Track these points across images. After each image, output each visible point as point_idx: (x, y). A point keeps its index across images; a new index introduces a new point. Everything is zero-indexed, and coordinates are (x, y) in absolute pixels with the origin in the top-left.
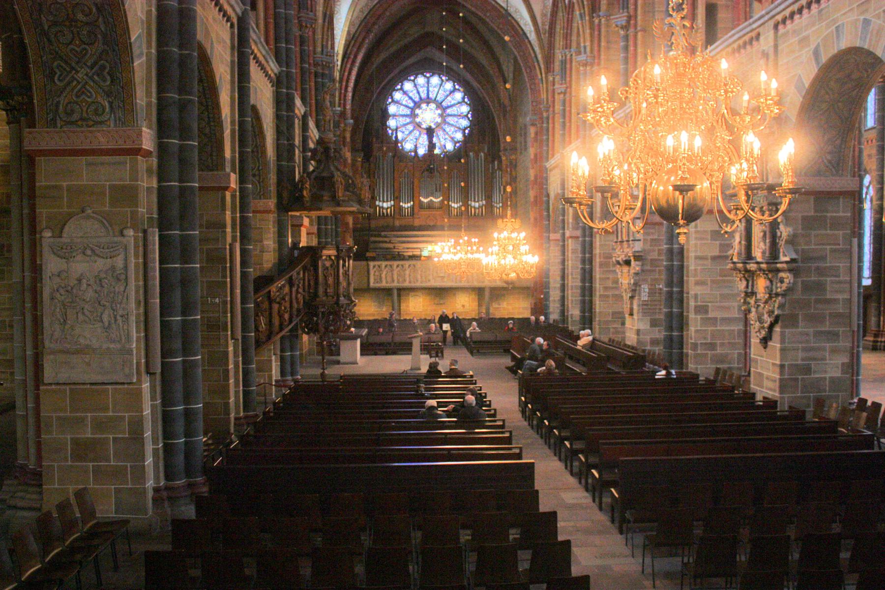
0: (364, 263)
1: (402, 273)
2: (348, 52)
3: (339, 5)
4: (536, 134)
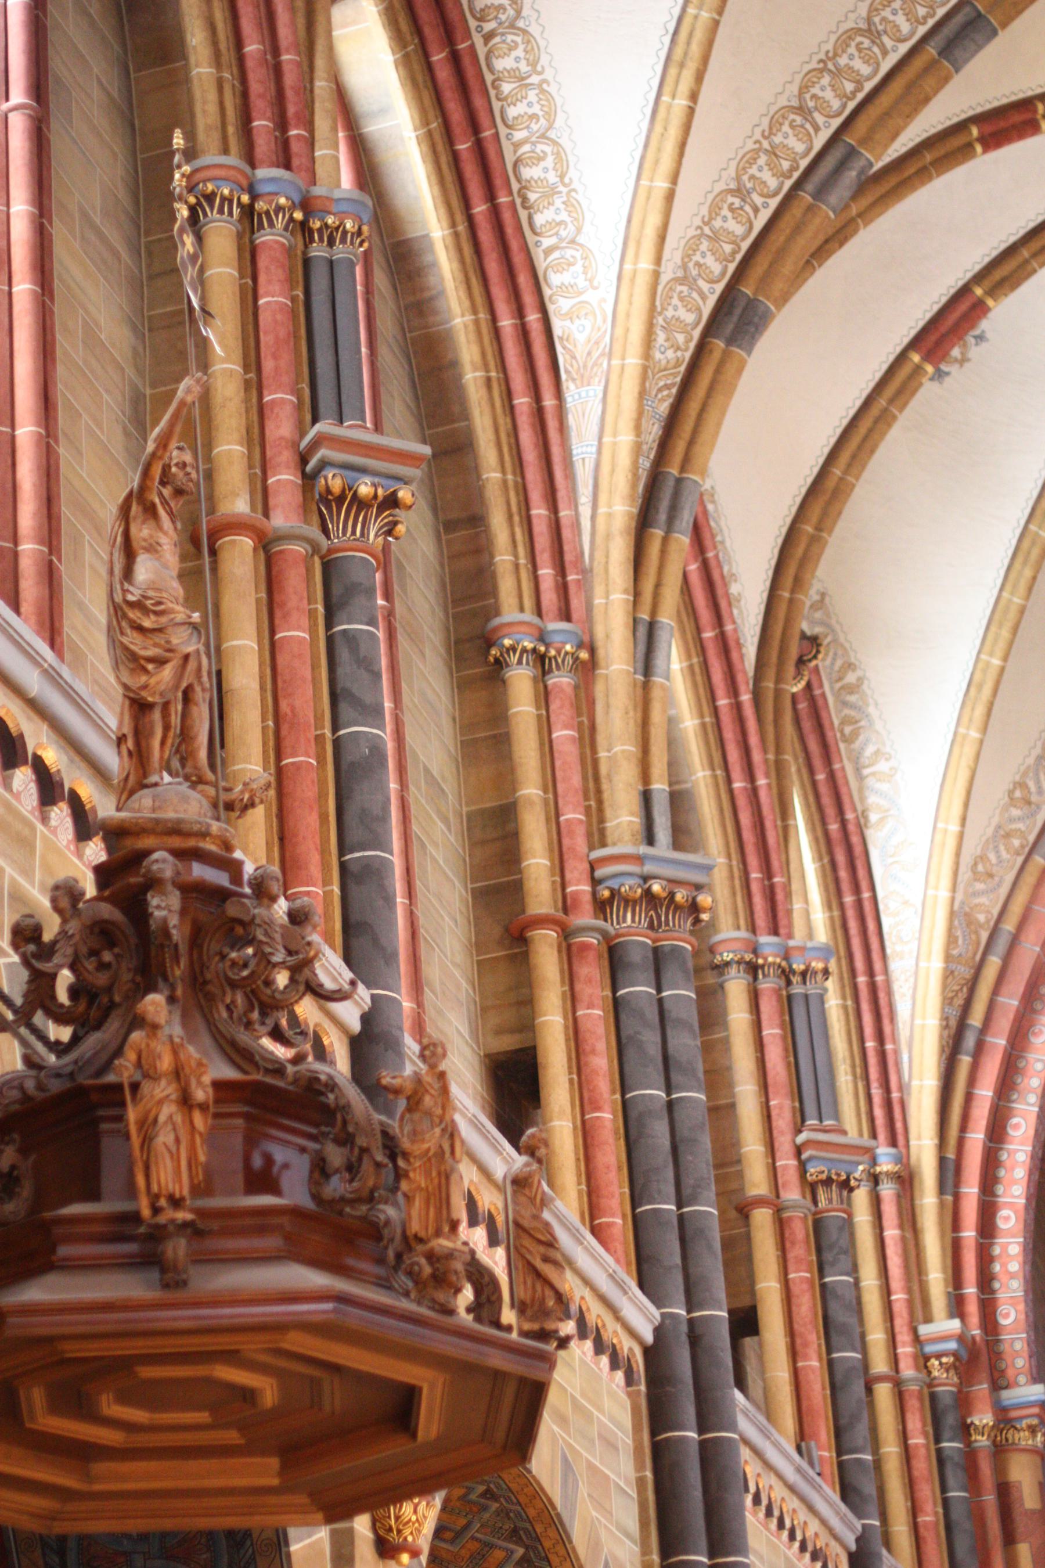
2: (976, 1020)
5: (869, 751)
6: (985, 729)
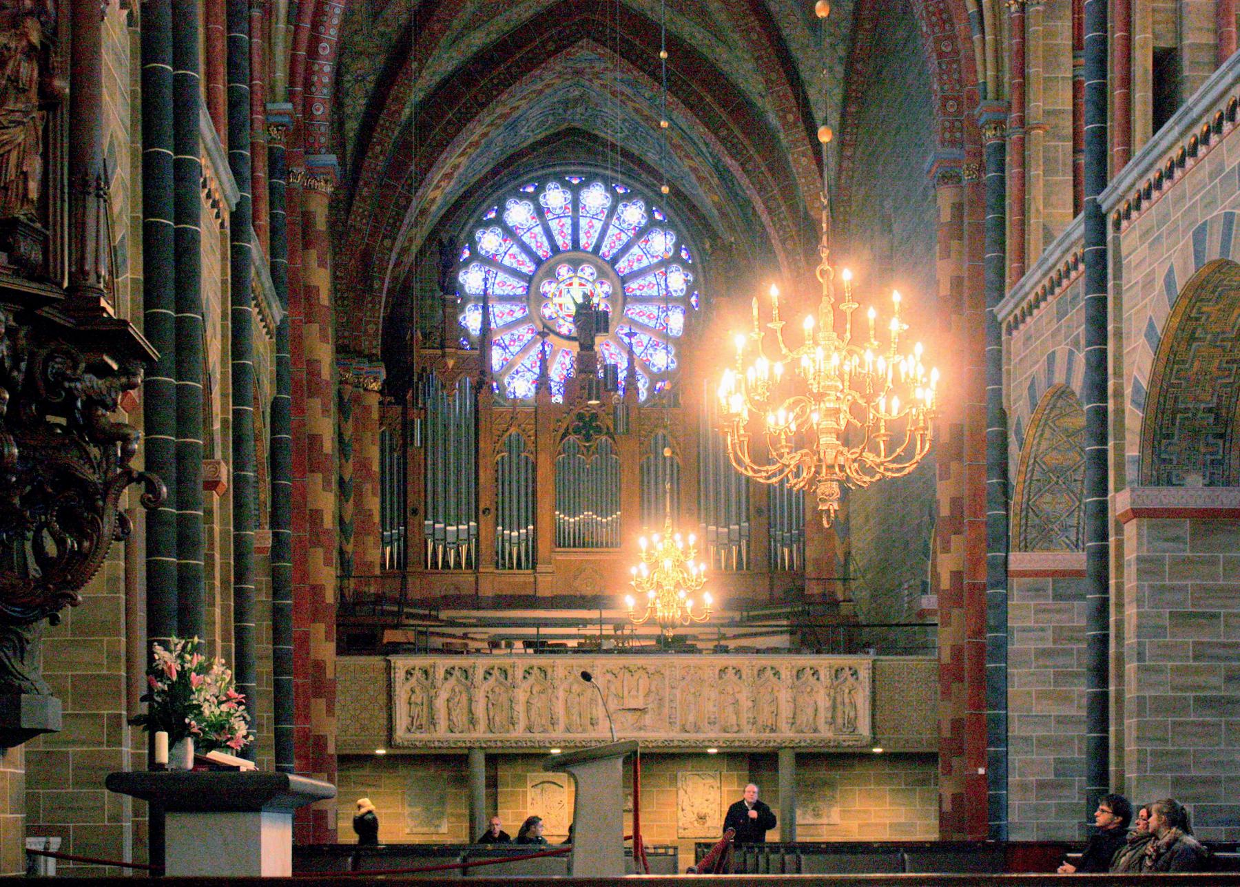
0: (377, 661)
1: (504, 698)
4: (958, 208)
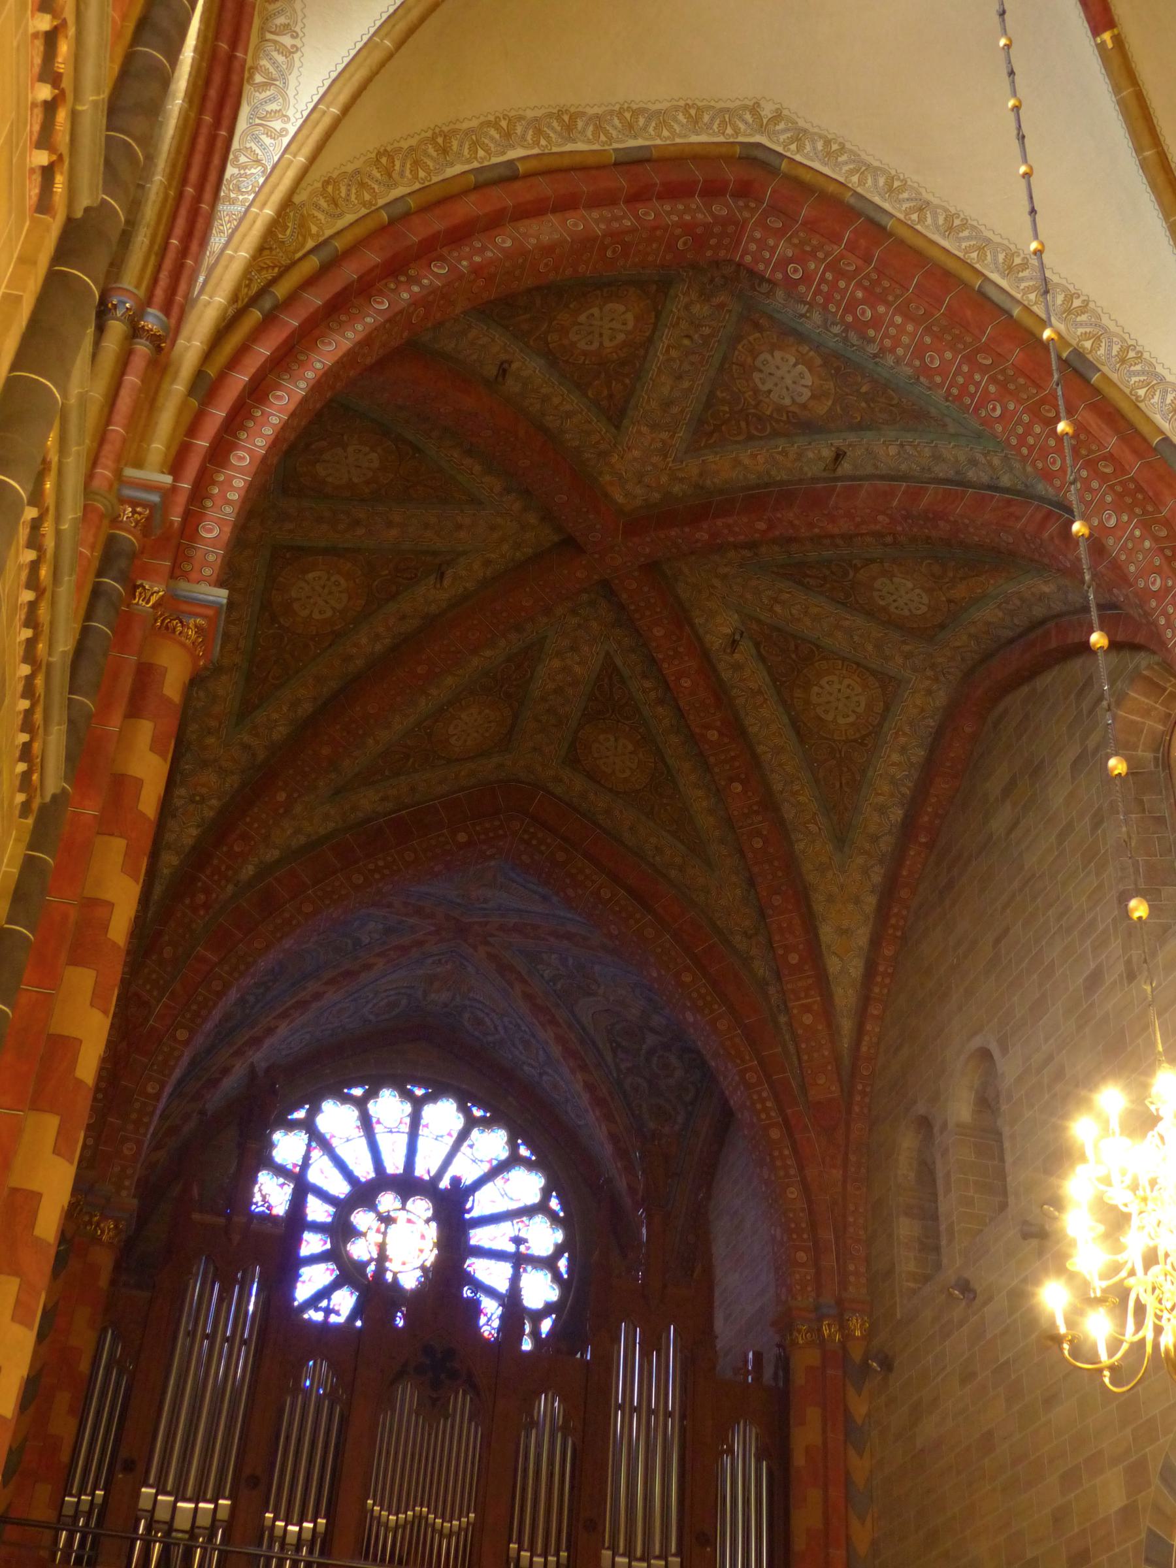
3: (289, 52)
5: (281, 20)
6: (400, 44)
